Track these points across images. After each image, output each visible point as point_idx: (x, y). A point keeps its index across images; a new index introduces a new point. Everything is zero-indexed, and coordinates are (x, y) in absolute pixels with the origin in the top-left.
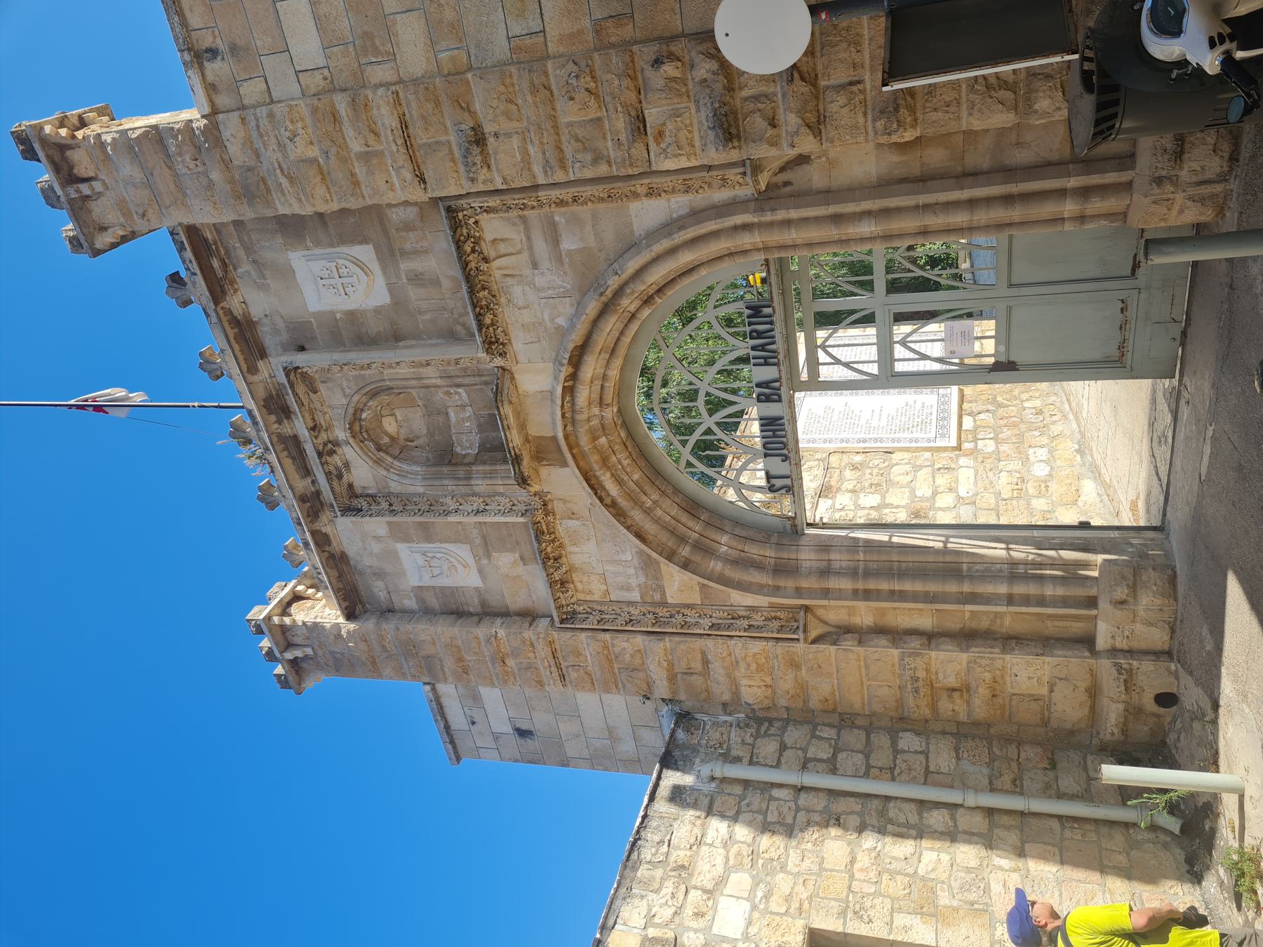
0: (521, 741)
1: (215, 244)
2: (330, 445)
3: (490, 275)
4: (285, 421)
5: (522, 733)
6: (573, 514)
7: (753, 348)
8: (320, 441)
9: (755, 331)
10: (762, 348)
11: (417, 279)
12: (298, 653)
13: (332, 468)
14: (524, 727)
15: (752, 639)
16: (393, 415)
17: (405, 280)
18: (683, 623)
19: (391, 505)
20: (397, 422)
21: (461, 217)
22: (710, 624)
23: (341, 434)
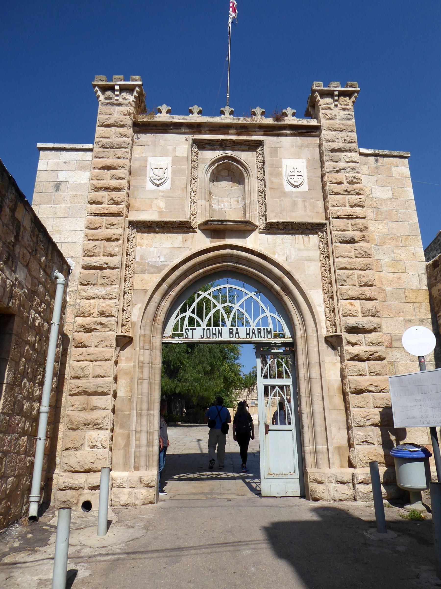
0: (53, 184)
5: (58, 186)
7: (253, 329)
9: (261, 332)
10: (254, 333)
11: (294, 204)
14: (61, 187)
16: (228, 175)
17: (294, 199)
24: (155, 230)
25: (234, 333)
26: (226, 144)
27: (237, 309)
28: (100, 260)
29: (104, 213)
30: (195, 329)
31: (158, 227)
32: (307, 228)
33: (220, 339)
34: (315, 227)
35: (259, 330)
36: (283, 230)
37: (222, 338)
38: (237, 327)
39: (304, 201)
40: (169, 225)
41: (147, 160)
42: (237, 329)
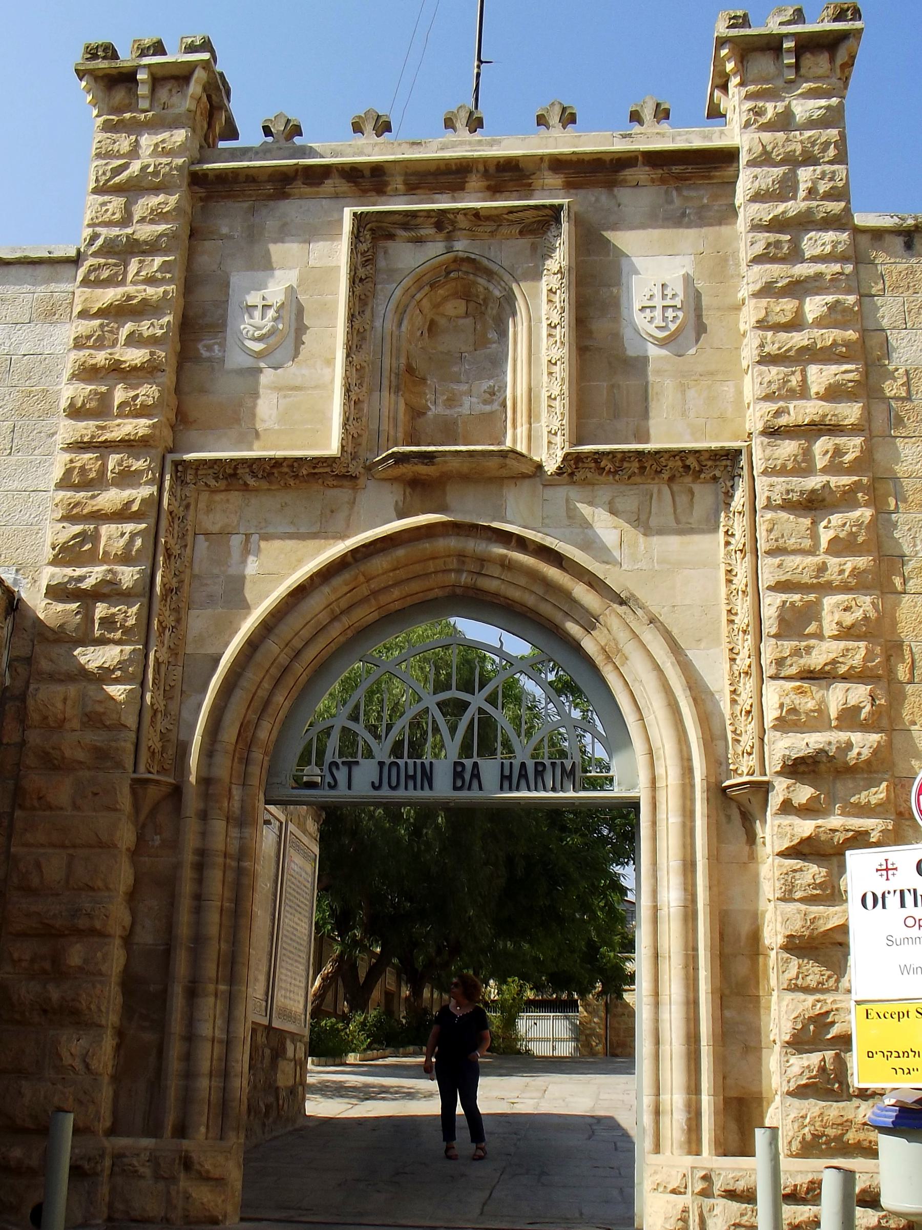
1: (710, 178)
2: (450, 228)
3: (653, 479)
4: (486, 183)
6: (332, 512)
7: (523, 765)
8: (460, 217)
12: (143, 90)
13: (419, 220)
15: (137, 712)
18: (164, 624)
19: (361, 280)
20: (457, 317)
21: (724, 463)
22: (160, 660)
23: (461, 245)
24: (246, 484)
25: (467, 777)
26: (453, 223)
27: (480, 708)
28: (94, 575)
29: (106, 441)
30: (357, 763)
31: (254, 474)
32: (687, 468)
33: (426, 793)
34: (710, 463)
35: (540, 768)
36: (616, 472)
37: (431, 788)
38: (475, 759)
39: (682, 385)
40: (285, 470)
41: (229, 283)
42: (475, 765)
